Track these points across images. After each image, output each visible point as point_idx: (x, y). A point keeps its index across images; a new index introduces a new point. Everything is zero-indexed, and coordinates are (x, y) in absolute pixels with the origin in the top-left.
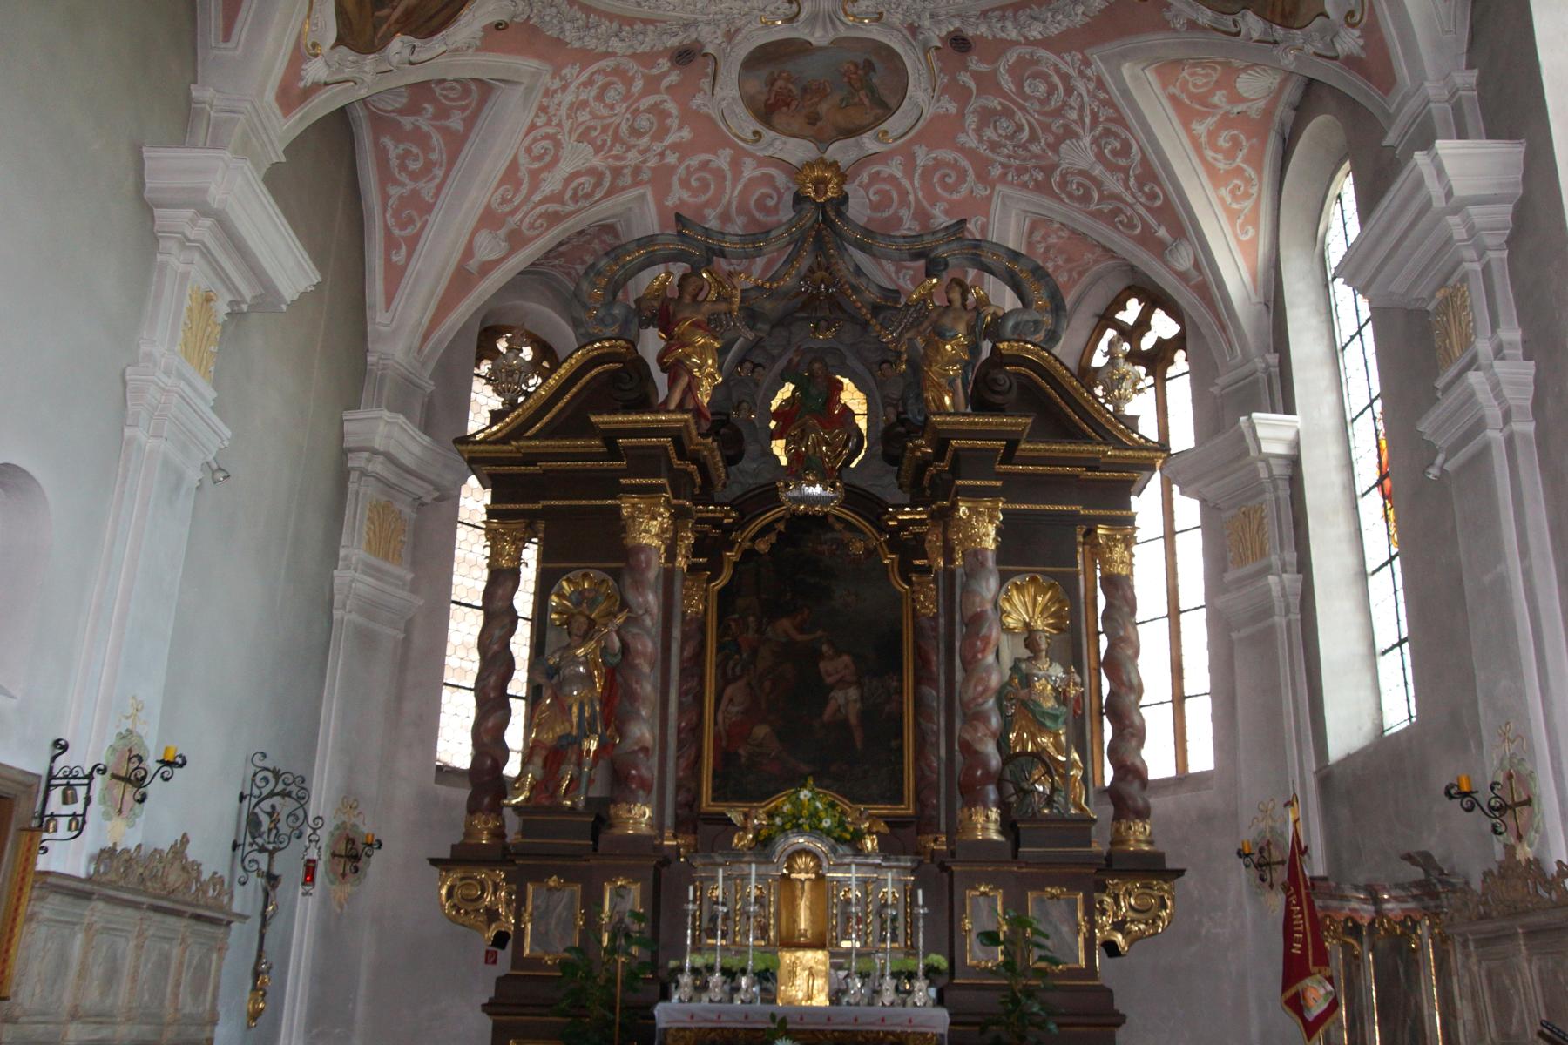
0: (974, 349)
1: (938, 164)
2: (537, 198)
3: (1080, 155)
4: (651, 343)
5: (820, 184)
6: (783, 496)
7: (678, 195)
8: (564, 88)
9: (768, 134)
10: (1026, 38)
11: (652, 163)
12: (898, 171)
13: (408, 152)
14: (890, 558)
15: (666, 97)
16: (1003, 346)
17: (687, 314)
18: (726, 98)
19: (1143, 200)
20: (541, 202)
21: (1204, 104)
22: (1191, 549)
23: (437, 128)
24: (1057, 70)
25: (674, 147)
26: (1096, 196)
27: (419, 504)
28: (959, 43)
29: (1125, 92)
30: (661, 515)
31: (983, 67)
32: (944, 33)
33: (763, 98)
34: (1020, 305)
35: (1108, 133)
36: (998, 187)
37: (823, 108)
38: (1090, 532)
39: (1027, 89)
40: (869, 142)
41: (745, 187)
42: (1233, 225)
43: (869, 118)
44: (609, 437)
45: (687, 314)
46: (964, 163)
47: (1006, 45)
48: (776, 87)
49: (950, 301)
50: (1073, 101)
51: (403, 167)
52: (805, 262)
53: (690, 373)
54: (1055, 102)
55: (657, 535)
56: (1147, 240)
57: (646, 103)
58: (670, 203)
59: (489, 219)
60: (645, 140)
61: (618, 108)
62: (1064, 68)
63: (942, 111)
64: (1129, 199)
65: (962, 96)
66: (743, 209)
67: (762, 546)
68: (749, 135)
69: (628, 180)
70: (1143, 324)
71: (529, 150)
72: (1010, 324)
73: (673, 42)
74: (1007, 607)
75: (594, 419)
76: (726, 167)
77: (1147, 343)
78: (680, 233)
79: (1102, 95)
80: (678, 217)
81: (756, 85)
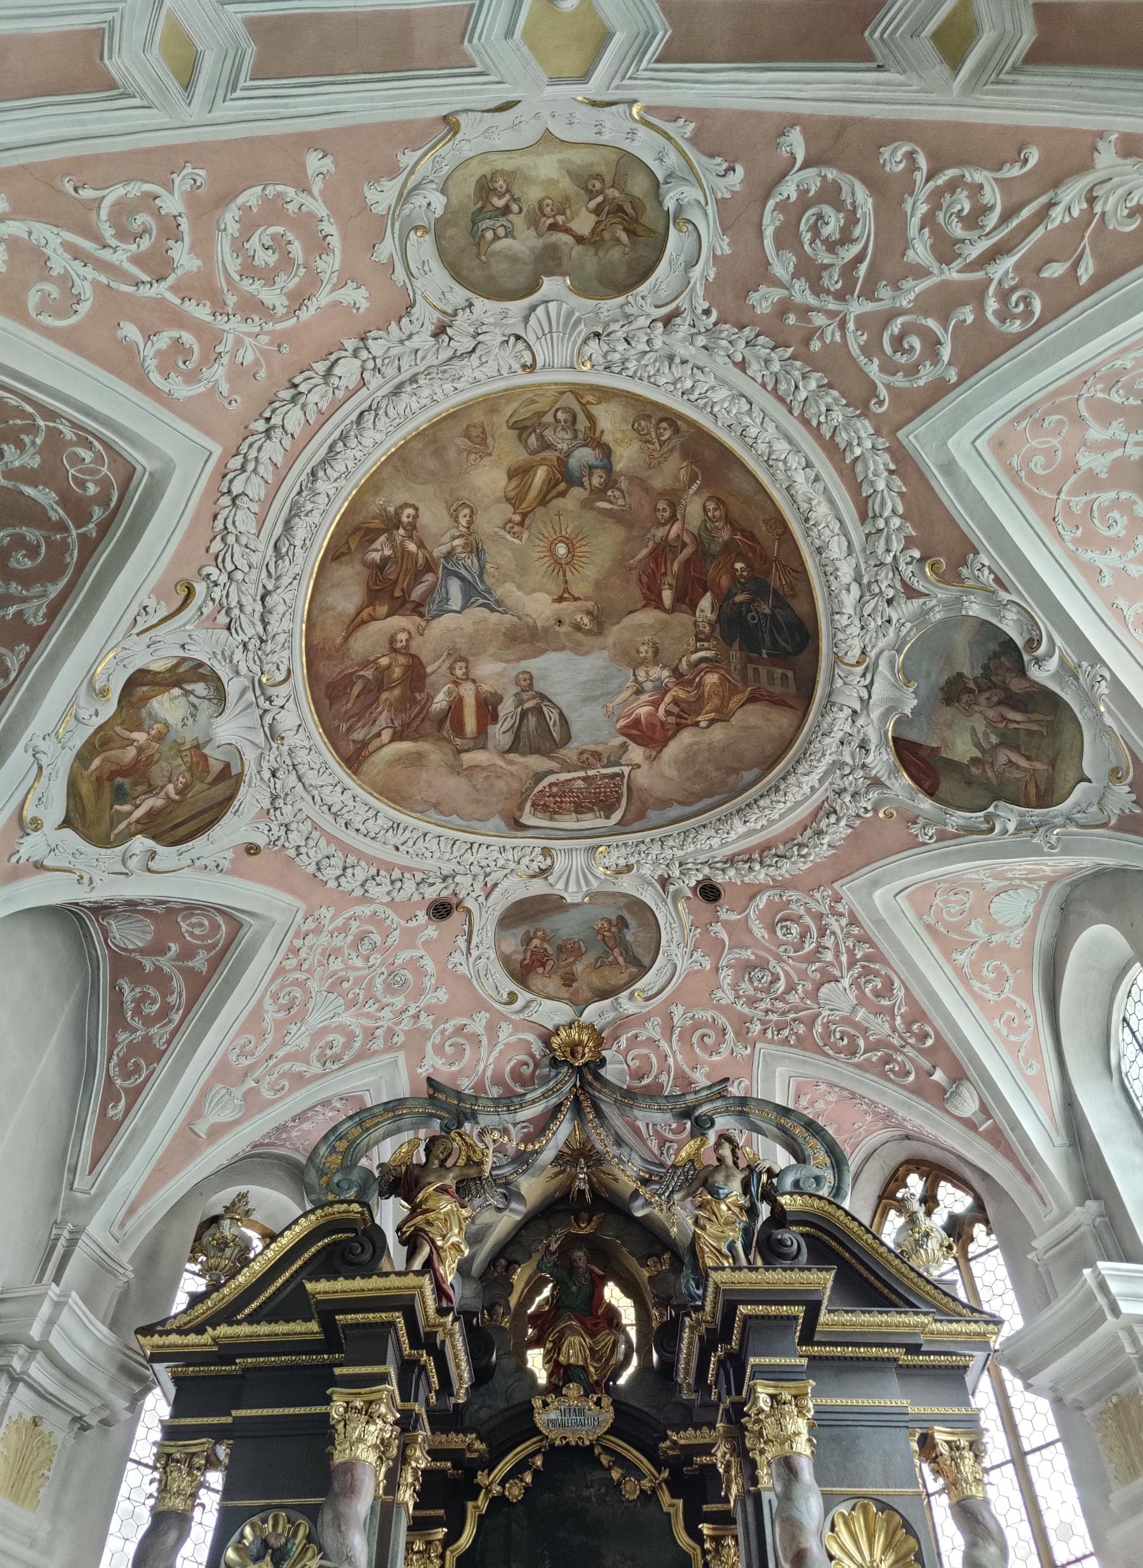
0: (752, 1212)
1: (697, 1025)
2: (280, 1054)
3: (840, 997)
4: (389, 1214)
5: (573, 1048)
6: (541, 1419)
7: (434, 1065)
8: (317, 931)
9: (524, 996)
10: (774, 880)
11: (406, 1024)
12: (655, 1027)
13: (145, 996)
14: (673, 1506)
15: (422, 952)
16: (785, 1200)
17: (431, 1179)
18: (483, 959)
19: (912, 1041)
20: (287, 1058)
21: (961, 933)
22: (1054, 1475)
23: (180, 969)
24: (808, 911)
25: (430, 1010)
26: (861, 1043)
27: (80, 1424)
28: (709, 892)
29: (880, 922)
30: (382, 1417)
31: (734, 917)
32: (693, 883)
33: (520, 957)
34: (793, 1161)
35: (867, 972)
36: (758, 1045)
37: (579, 968)
38: (926, 1443)
39: (779, 933)
40: (627, 1004)
41: (501, 1052)
42: (1016, 1059)
43: (625, 977)
44: (326, 1312)
45: (431, 1179)
46: (722, 1020)
47: (755, 891)
48: (531, 947)
49: (720, 1160)
50: (829, 942)
51: (137, 1011)
52: (563, 1130)
53: (433, 1242)
54: (809, 947)
55: (375, 1446)
56: (923, 1090)
57: (404, 956)
58: (423, 1071)
59: (223, 1073)
60: (399, 1001)
61: (372, 961)
62: (815, 907)
63: (697, 967)
64: (896, 1041)
65: (716, 948)
66: (498, 1081)
67: (515, 1492)
68: (505, 996)
69: (378, 1045)
70: (930, 1201)
71: (275, 997)
72: (788, 1182)
73: (431, 893)
74: (835, 1550)
75: (310, 1286)
76: (480, 1030)
78: (431, 1097)
79: (856, 931)
80: (429, 1080)
81: (512, 944)
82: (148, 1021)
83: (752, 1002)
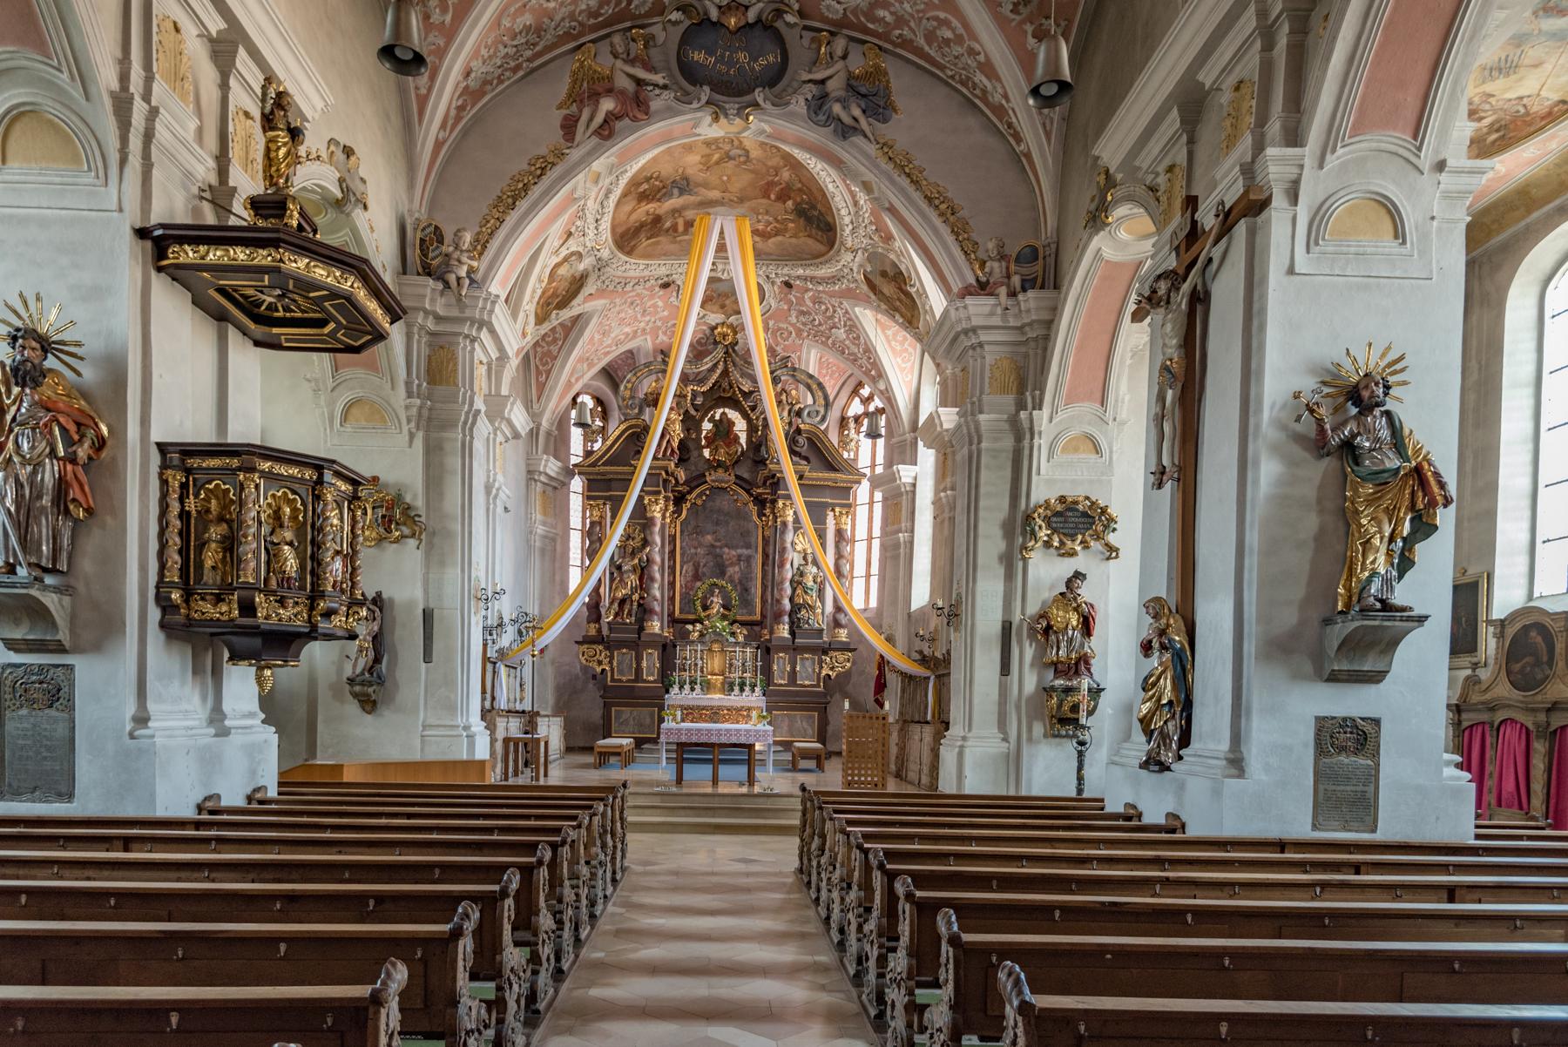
1: (780, 329)
5: (725, 336)
65: (790, 303)
70: (870, 399)
77: (871, 408)
82: (548, 344)
83: (804, 324)
